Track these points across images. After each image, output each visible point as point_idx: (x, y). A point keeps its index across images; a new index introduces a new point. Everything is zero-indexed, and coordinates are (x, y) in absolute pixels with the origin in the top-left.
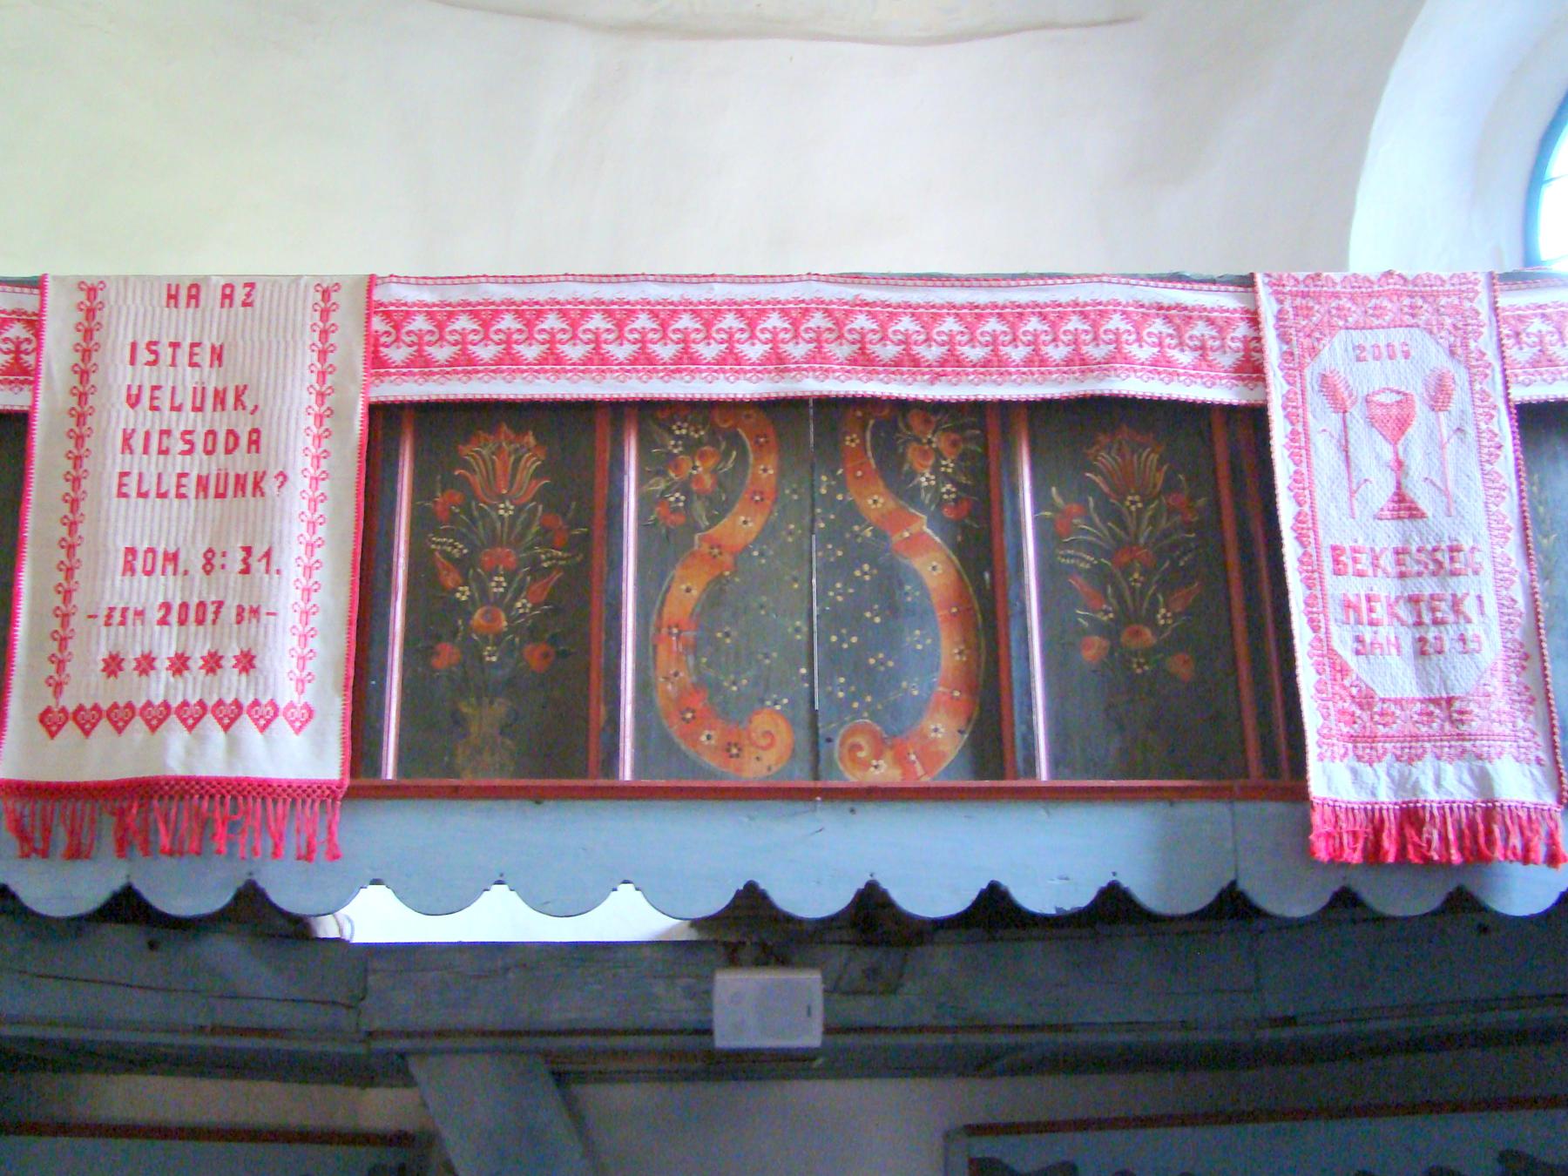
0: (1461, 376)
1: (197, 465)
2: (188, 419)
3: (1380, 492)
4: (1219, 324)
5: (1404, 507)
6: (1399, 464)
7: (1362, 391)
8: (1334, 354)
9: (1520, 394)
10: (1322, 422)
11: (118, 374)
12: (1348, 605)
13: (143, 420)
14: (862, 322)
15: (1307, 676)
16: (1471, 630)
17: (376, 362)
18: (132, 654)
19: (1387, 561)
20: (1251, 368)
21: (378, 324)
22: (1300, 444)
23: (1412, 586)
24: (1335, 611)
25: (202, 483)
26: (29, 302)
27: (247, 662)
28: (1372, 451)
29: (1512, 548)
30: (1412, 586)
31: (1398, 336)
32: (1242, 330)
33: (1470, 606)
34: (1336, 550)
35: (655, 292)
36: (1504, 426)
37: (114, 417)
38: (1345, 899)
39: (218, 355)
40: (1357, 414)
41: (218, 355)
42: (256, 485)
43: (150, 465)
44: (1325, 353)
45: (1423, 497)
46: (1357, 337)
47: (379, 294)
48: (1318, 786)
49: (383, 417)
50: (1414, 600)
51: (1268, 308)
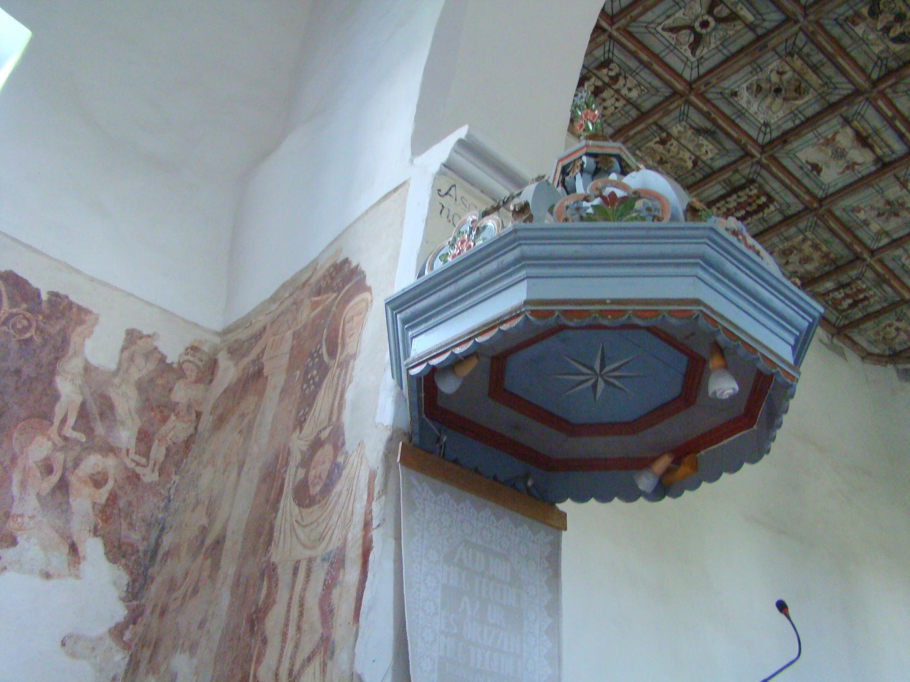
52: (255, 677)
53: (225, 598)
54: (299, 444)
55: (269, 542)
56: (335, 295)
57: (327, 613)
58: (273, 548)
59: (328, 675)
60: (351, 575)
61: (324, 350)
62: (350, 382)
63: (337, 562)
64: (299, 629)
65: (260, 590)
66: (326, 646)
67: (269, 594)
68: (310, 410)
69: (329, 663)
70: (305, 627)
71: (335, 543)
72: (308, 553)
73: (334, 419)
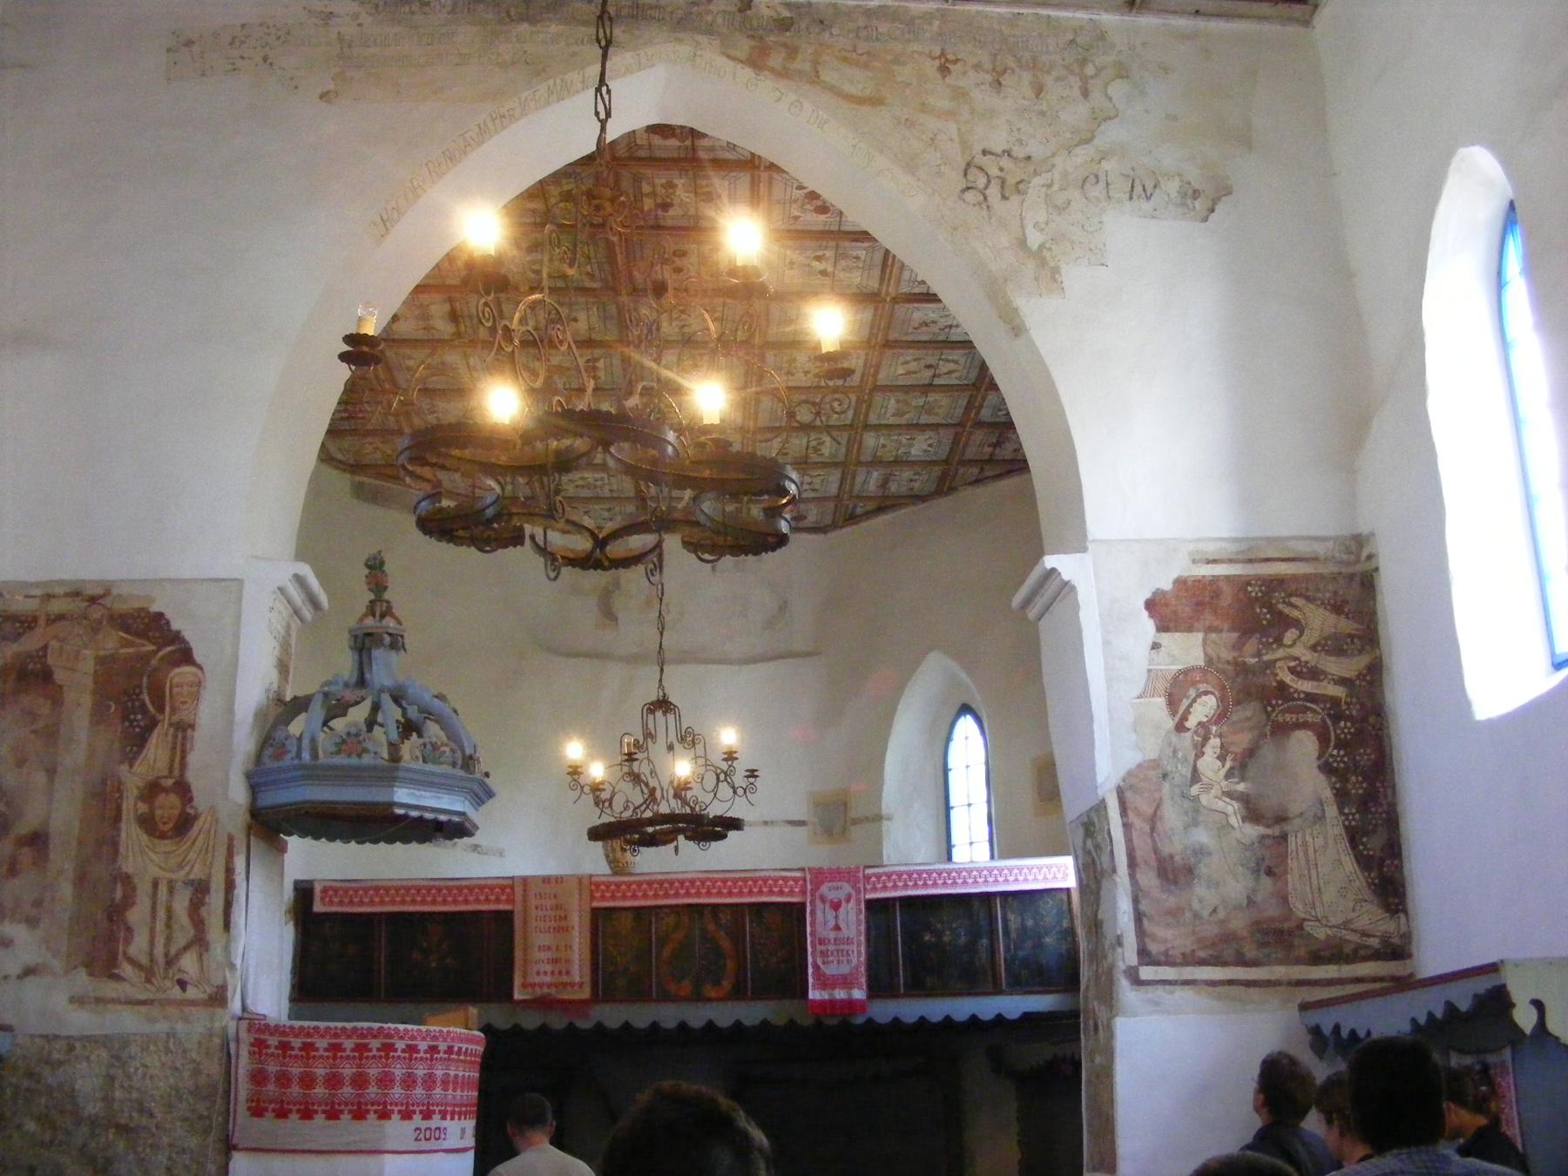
0: (854, 895)
1: (553, 924)
2: (550, 912)
3: (832, 923)
4: (796, 880)
5: (837, 928)
6: (836, 917)
7: (830, 898)
8: (824, 889)
9: (870, 896)
10: (818, 903)
11: (533, 902)
12: (822, 952)
13: (540, 913)
14: (708, 883)
15: (810, 971)
16: (851, 958)
17: (592, 898)
18: (542, 970)
19: (832, 941)
20: (803, 892)
21: (593, 887)
22: (813, 912)
23: (838, 947)
24: (818, 954)
25: (554, 929)
26: (510, 882)
27: (568, 973)
28: (830, 914)
29: (863, 938)
30: (838, 947)
31: (840, 884)
32: (801, 882)
33: (850, 952)
34: (820, 939)
35: (660, 877)
36: (863, 906)
37: (534, 913)
38: (819, 1023)
39: (555, 897)
40: (827, 905)
41: (555, 897)
42: (567, 930)
43: (541, 924)
44: (821, 889)
45: (842, 925)
46: (830, 884)
47: (593, 879)
48: (811, 996)
49: (595, 911)
50: (838, 951)
51: (808, 877)
52: (125, 953)
53: (66, 890)
54: (133, 778)
55: (116, 852)
56: (152, 648)
57: (199, 924)
58: (120, 861)
59: (205, 963)
60: (216, 899)
61: (146, 698)
62: (192, 749)
63: (200, 890)
64: (168, 926)
65: (113, 890)
66: (200, 941)
67: (125, 897)
68: (139, 752)
69: (205, 956)
70: (175, 927)
71: (197, 873)
72: (169, 875)
73: (176, 772)
